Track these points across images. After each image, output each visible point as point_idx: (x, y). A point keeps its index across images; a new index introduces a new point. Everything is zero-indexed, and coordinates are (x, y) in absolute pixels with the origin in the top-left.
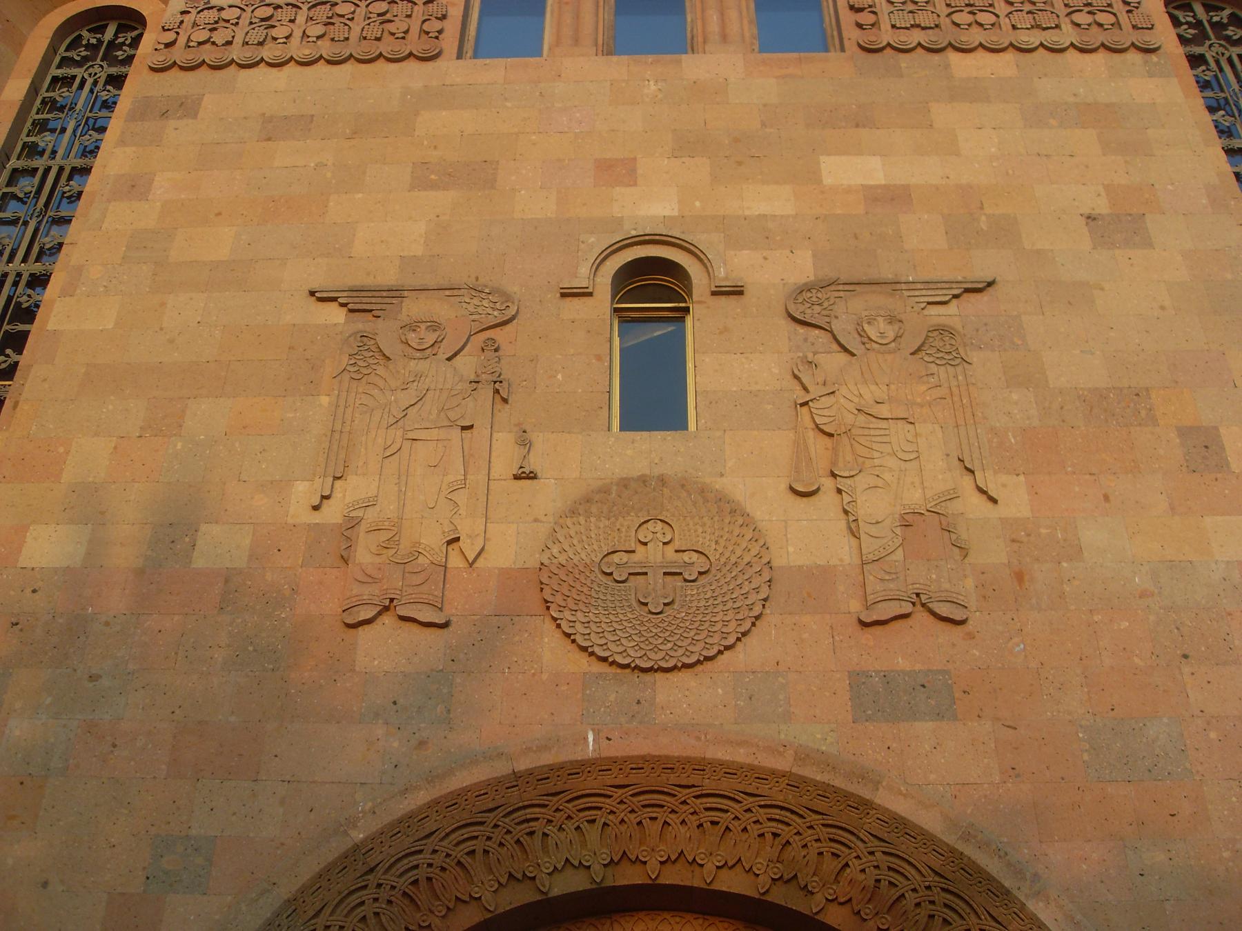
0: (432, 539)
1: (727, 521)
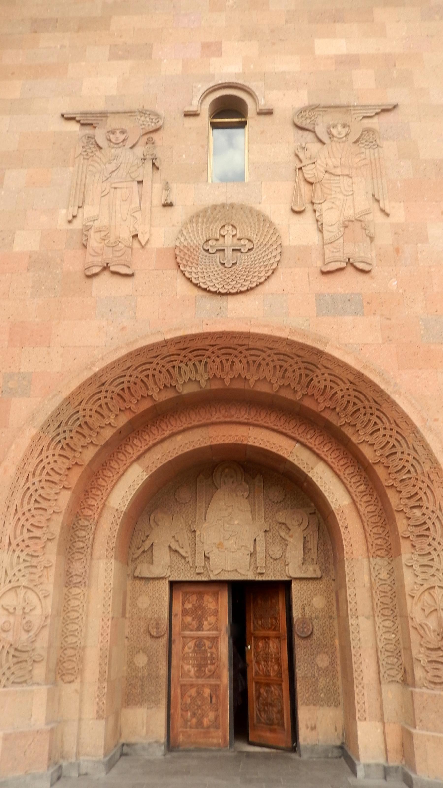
0: (126, 235)
1: (262, 225)
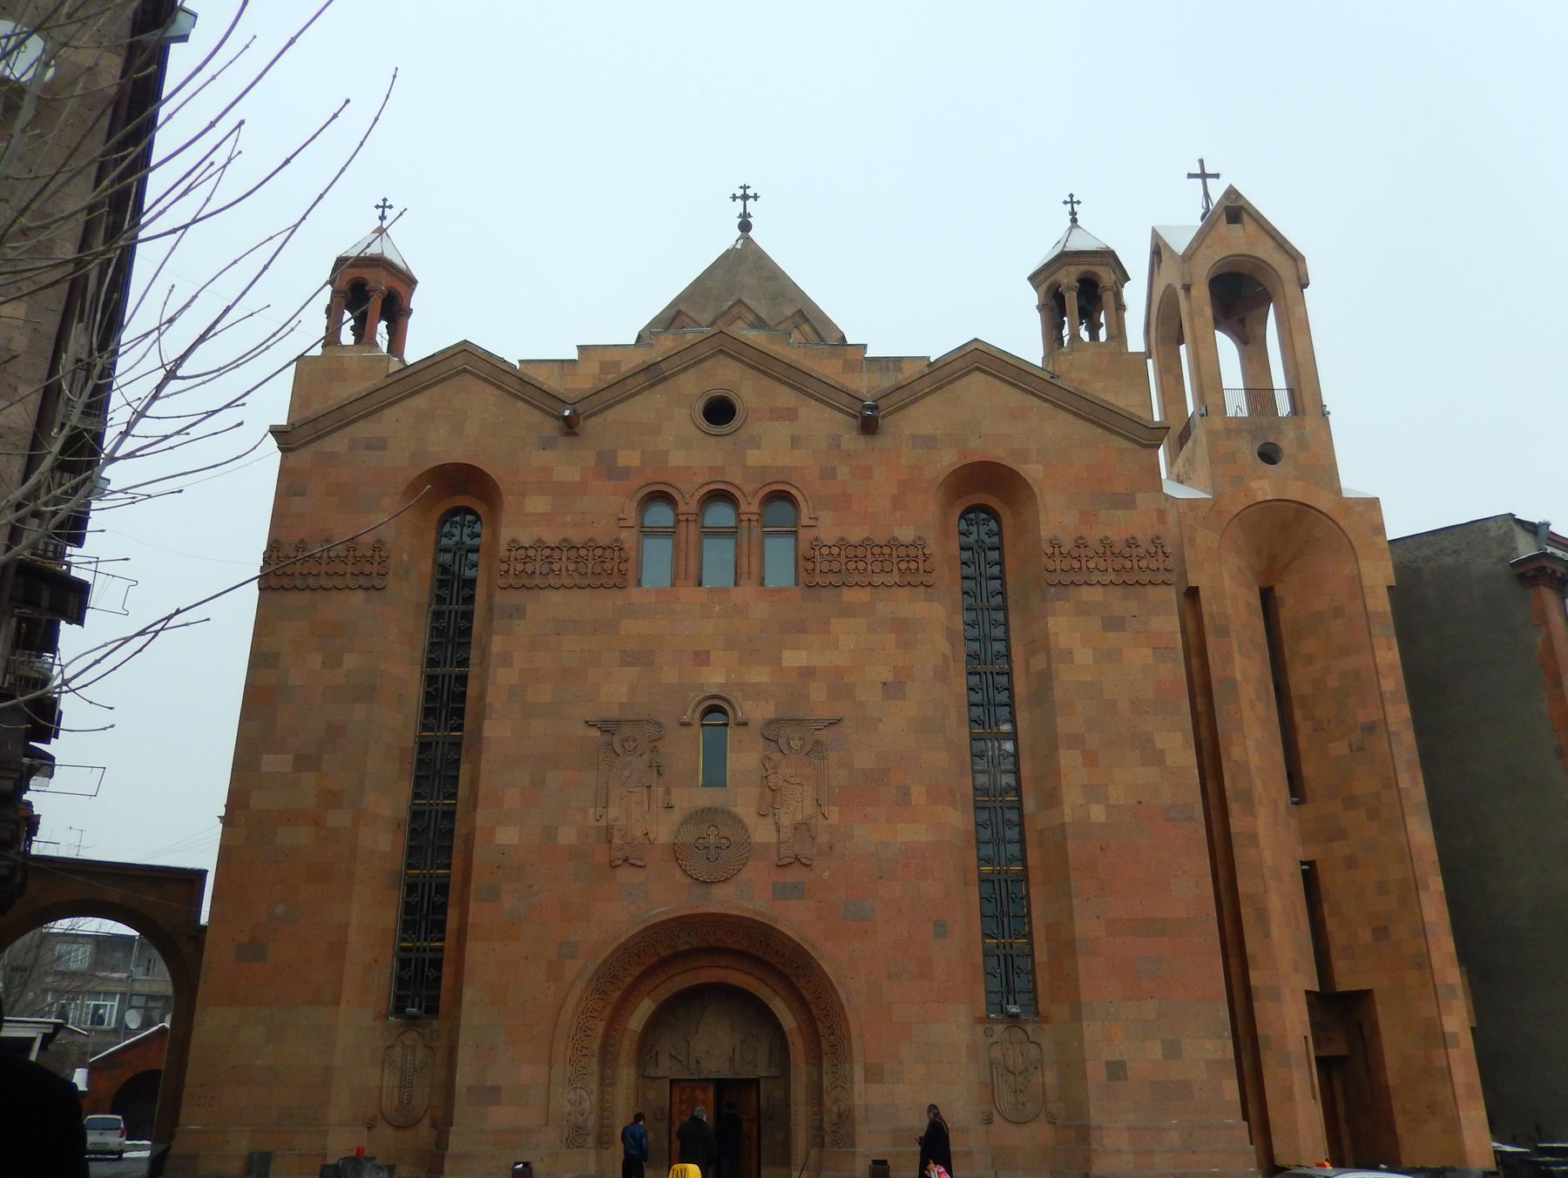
0: (639, 833)
